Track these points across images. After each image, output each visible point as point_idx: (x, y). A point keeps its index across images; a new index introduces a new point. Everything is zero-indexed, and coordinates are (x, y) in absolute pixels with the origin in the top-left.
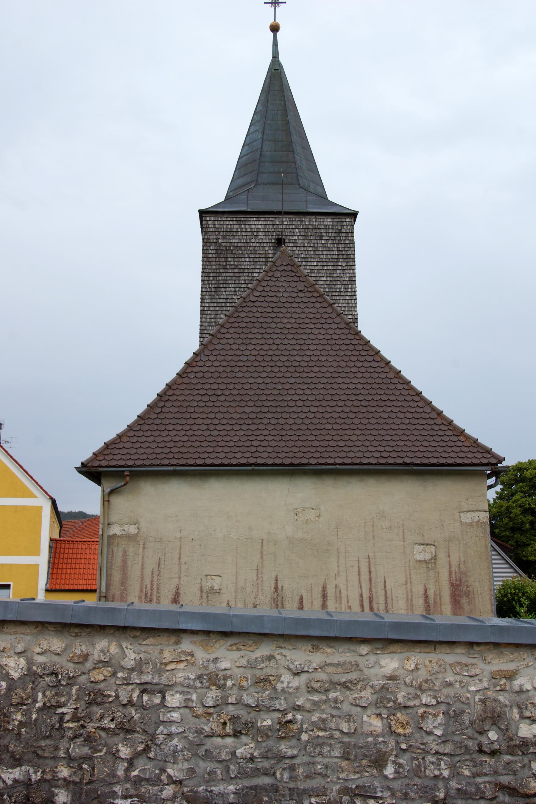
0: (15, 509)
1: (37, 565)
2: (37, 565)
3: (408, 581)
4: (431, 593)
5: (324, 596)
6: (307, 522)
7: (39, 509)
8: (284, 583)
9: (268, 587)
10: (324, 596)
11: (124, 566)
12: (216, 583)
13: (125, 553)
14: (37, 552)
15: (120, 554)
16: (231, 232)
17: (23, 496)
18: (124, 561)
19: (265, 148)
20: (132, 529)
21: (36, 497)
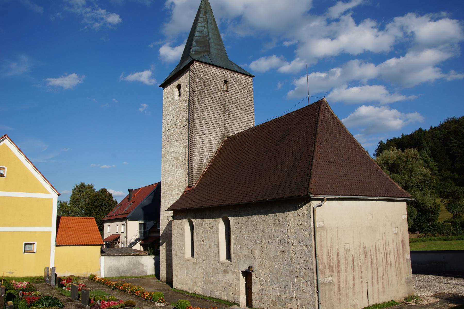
0: (38, 199)
1: (50, 232)
2: (50, 232)
3: (393, 242)
4: (398, 245)
5: (376, 249)
6: (370, 219)
7: (51, 200)
8: (366, 245)
9: (362, 247)
10: (376, 249)
11: (321, 242)
12: (348, 247)
13: (321, 235)
14: (50, 225)
15: (319, 236)
16: (205, 73)
17: (43, 192)
18: (321, 239)
19: (210, 36)
20: (322, 225)
21: (49, 193)
